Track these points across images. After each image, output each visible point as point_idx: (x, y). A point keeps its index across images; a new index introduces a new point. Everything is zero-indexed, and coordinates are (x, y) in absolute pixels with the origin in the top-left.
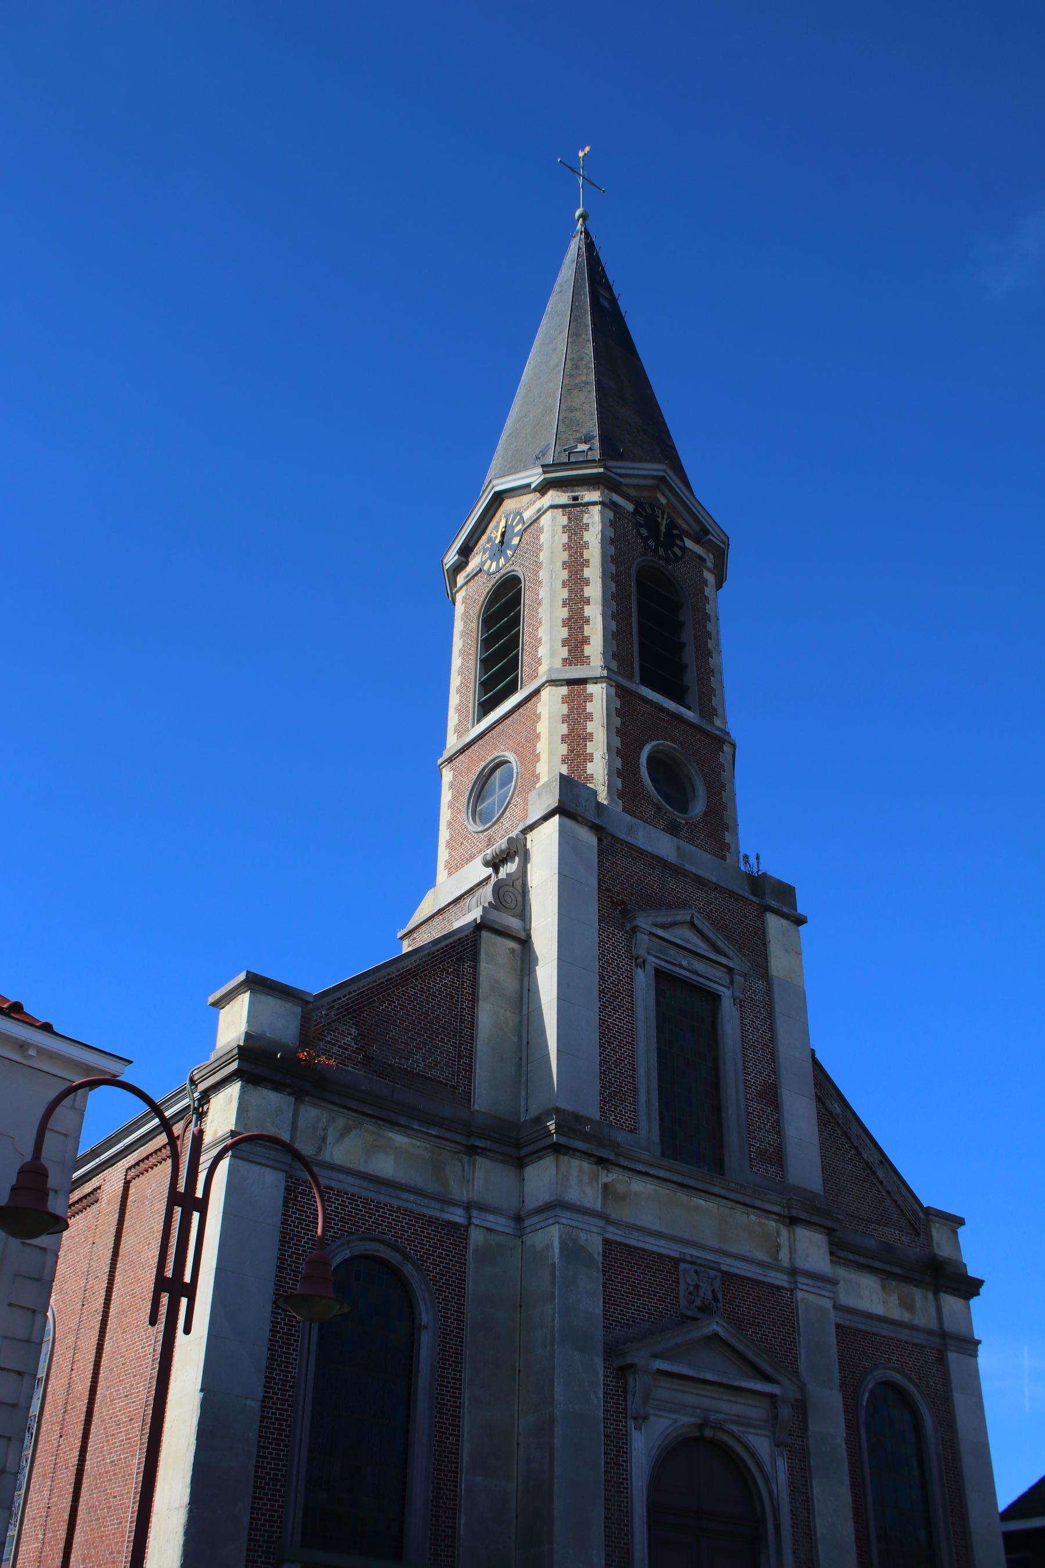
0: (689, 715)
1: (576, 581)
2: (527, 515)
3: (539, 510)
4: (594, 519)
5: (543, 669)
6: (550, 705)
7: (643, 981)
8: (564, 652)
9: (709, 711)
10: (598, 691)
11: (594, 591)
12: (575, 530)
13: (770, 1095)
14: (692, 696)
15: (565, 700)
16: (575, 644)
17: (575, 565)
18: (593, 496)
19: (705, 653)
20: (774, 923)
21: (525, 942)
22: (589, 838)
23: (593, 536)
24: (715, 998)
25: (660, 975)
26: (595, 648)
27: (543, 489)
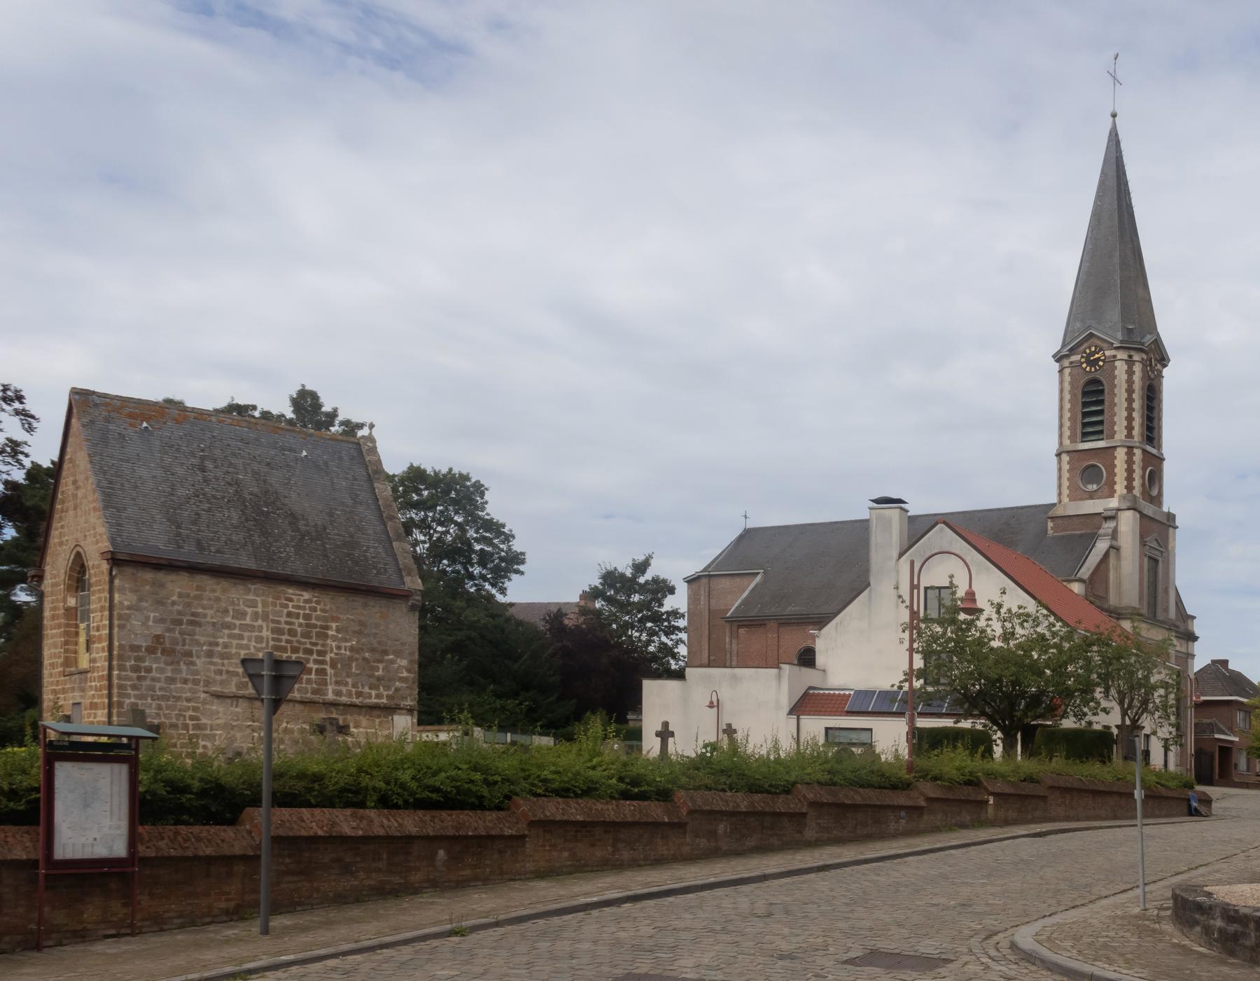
0: (1154, 451)
1: (1130, 400)
2: (1108, 353)
3: (1115, 356)
4: (1137, 368)
5: (1117, 437)
6: (1121, 454)
7: (1146, 559)
8: (1125, 432)
9: (1159, 447)
10: (1138, 452)
11: (1136, 405)
12: (1130, 373)
13: (1166, 591)
14: (1155, 442)
15: (1127, 454)
16: (1130, 428)
17: (1130, 391)
18: (1136, 357)
19: (1160, 419)
20: (1171, 530)
21: (1118, 549)
22: (1138, 516)
23: (1137, 377)
24: (1157, 561)
25: (1150, 558)
26: (1136, 432)
27: (1117, 348)
